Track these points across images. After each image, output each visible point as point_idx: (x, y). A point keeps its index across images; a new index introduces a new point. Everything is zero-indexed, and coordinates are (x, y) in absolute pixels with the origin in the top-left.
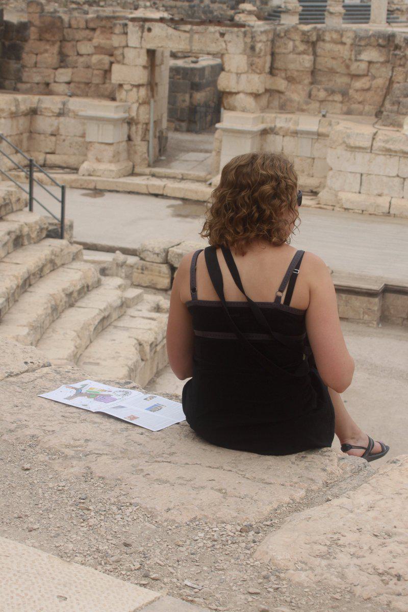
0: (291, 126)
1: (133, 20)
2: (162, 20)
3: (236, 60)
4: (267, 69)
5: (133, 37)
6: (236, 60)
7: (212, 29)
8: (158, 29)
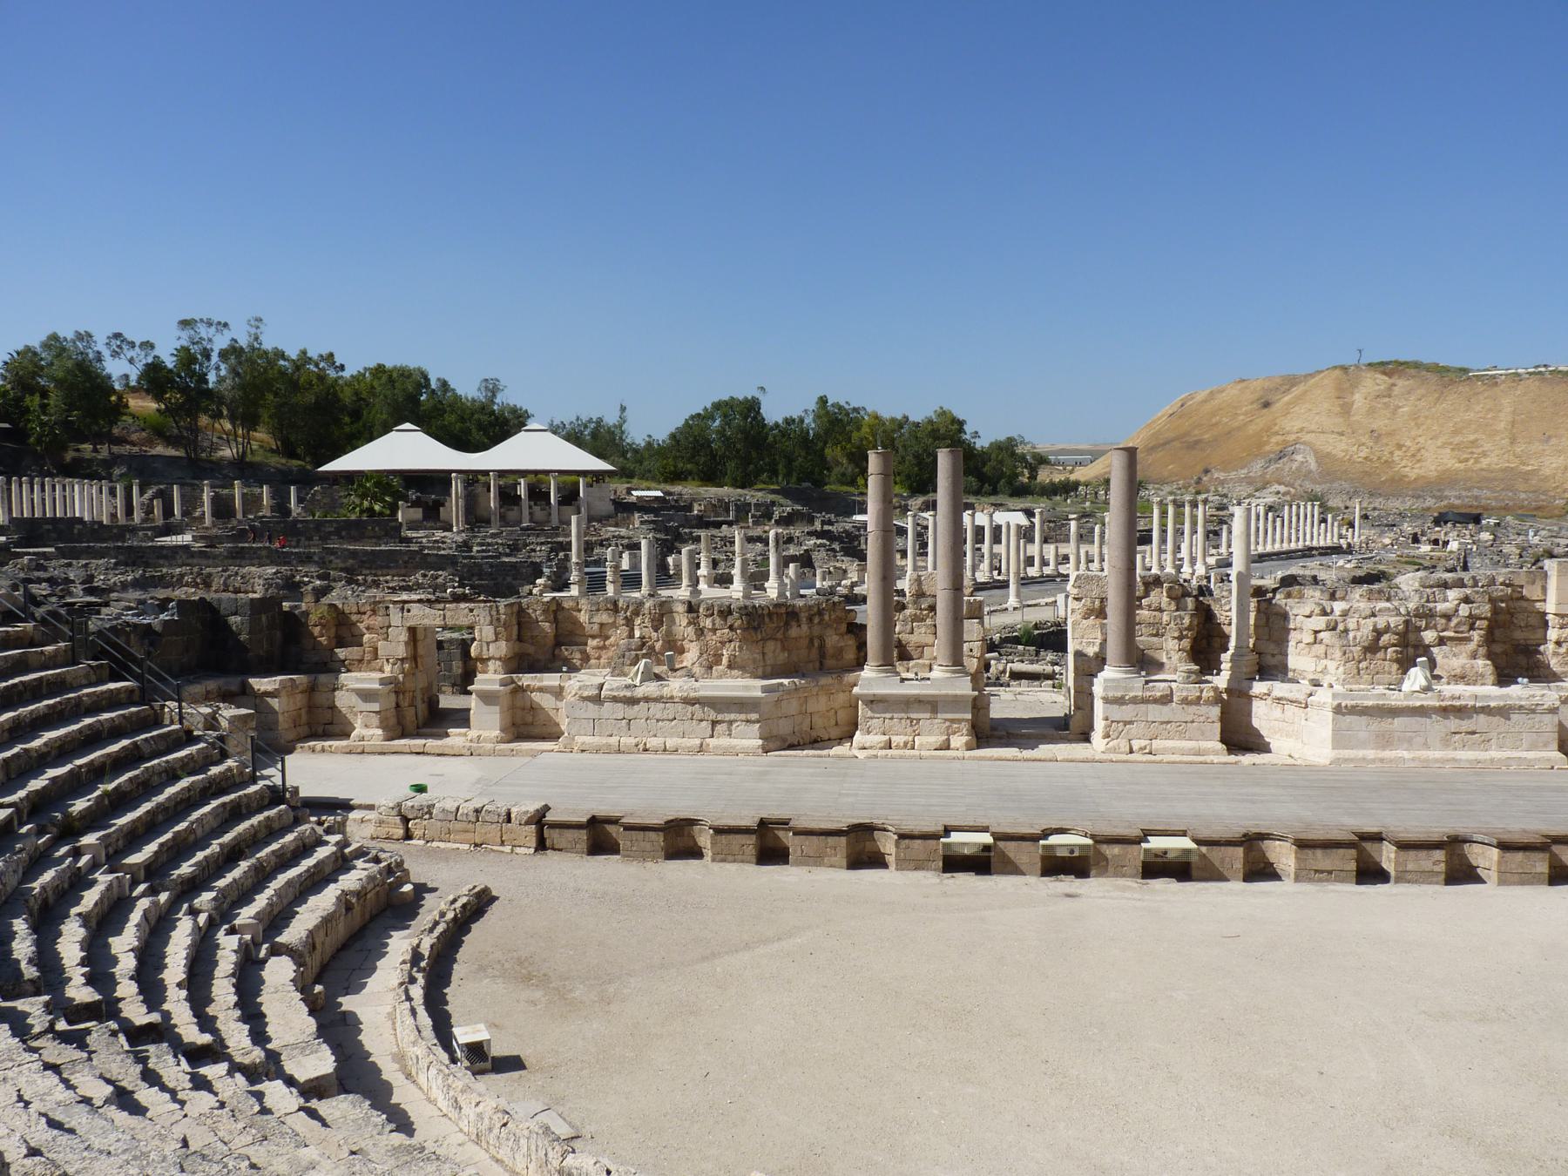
0: (538, 684)
1: (395, 602)
2: (420, 601)
3: (485, 631)
4: (515, 636)
5: (395, 617)
6: (485, 631)
7: (463, 605)
8: (415, 608)
